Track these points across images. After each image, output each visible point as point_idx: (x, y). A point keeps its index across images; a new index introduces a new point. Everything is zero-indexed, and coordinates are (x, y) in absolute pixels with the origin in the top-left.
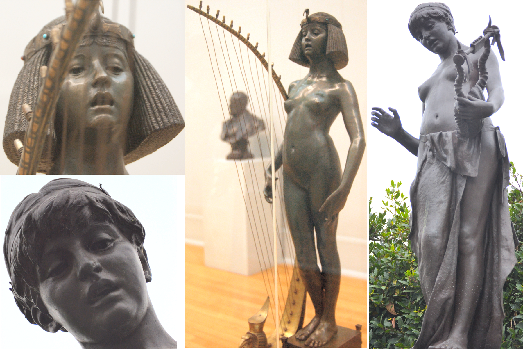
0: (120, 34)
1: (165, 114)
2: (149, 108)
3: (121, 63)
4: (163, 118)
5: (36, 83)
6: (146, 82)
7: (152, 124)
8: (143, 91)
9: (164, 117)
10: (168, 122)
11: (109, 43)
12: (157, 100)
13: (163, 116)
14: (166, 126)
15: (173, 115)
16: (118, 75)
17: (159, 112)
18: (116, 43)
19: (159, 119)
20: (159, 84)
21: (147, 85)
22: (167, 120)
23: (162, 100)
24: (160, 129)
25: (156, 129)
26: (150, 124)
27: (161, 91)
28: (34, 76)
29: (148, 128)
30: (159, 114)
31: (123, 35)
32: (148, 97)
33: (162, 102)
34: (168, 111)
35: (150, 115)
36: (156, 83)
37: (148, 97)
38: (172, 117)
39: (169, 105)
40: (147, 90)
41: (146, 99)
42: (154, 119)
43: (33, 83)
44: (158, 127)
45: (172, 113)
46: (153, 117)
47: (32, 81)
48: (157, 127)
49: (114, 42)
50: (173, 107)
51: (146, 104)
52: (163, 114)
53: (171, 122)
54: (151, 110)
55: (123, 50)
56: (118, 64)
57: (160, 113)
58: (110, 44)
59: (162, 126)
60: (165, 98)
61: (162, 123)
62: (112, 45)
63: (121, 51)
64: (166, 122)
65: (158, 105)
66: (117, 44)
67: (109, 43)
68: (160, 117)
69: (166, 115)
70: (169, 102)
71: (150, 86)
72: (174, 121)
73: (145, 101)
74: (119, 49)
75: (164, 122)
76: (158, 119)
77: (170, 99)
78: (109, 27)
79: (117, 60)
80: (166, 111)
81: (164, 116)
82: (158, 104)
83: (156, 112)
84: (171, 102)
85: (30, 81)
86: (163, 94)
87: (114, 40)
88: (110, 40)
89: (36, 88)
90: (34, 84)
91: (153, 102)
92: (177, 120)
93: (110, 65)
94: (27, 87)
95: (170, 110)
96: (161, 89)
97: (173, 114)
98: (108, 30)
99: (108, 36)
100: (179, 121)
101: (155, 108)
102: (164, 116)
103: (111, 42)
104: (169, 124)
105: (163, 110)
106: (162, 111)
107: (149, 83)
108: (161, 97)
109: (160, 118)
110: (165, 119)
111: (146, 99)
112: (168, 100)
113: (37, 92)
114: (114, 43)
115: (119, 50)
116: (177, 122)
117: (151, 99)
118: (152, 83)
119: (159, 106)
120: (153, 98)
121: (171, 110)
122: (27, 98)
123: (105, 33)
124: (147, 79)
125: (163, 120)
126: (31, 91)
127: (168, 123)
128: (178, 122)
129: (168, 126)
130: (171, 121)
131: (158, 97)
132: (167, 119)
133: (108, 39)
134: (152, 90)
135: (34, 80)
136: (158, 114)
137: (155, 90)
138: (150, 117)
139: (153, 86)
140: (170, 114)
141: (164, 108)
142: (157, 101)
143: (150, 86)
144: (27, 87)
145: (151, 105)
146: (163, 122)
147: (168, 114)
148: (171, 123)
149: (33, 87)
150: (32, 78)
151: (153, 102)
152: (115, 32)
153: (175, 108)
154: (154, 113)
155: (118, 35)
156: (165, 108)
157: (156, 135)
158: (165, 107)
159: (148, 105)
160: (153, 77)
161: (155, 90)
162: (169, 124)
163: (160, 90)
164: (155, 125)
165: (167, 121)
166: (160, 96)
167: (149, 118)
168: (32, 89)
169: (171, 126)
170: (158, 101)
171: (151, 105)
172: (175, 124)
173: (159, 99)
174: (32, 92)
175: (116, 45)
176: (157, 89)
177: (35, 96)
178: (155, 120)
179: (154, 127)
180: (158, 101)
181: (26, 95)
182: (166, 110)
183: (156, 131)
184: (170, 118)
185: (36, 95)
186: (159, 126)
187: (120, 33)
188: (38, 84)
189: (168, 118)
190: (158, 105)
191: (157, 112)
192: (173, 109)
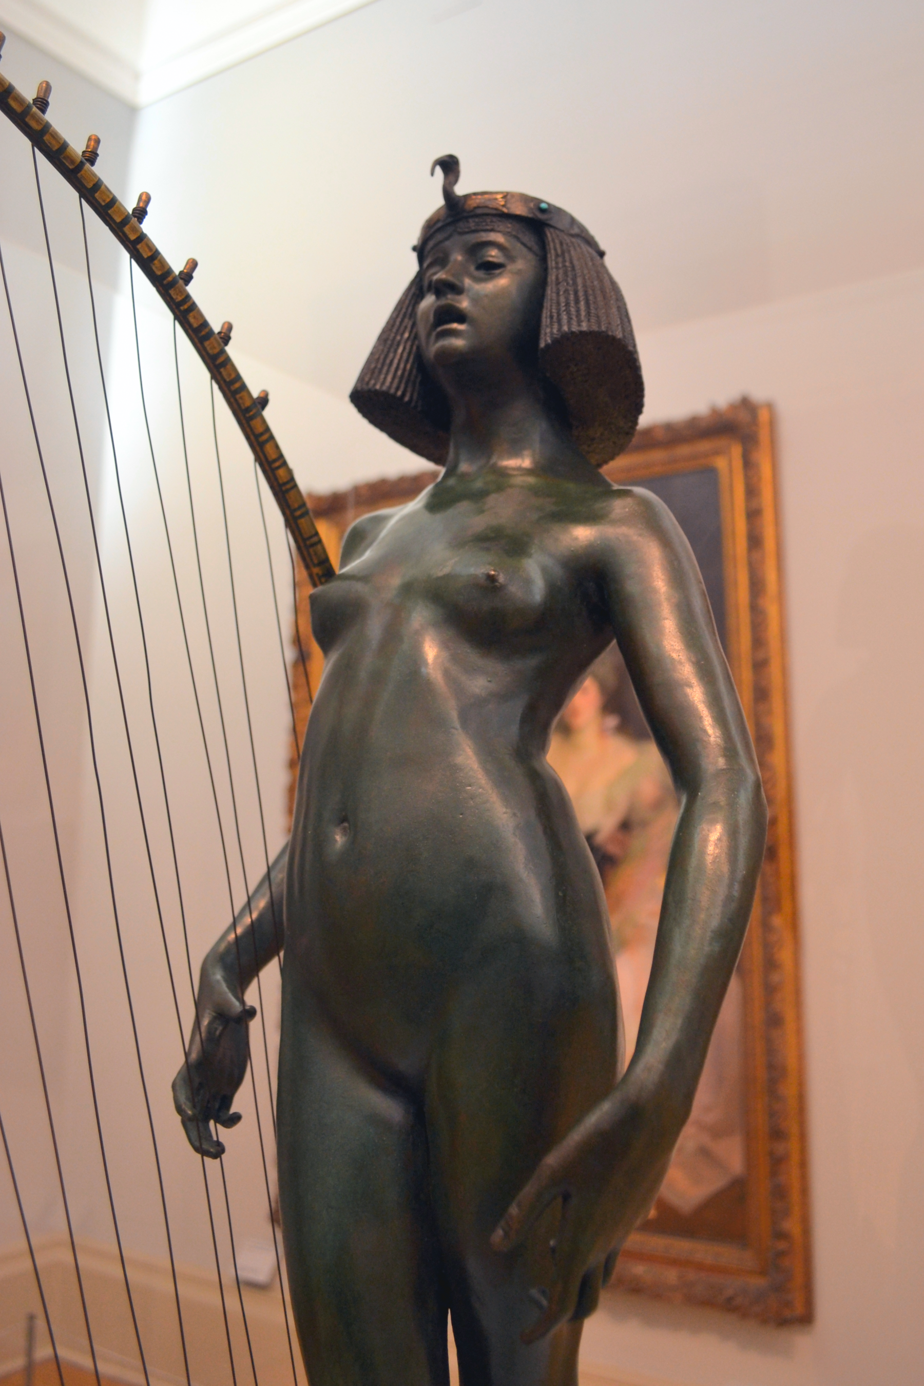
0: (501, 208)
55: (509, 232)
99: (477, 216)
123: (472, 211)
155: (496, 209)
175: (492, 227)
187: (503, 206)
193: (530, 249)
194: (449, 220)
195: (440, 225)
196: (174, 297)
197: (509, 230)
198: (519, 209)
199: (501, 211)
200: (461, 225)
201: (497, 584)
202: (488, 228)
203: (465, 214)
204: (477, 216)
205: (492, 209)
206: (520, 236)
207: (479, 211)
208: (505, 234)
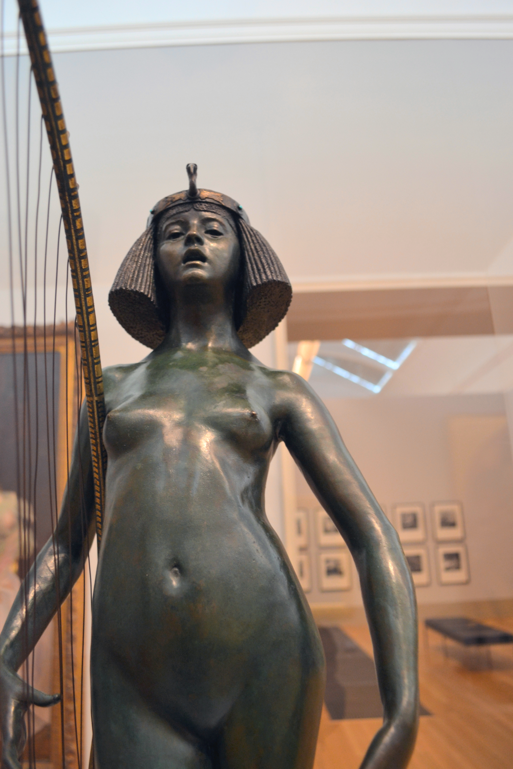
0: (221, 202)
6: (250, 246)
18: (216, 209)
21: (251, 249)
24: (258, 285)
32: (250, 259)
37: (250, 259)
40: (250, 253)
55: (224, 216)
73: (247, 263)
74: (219, 215)
87: (214, 207)
93: (208, 229)
107: (253, 247)
118: (255, 247)
120: (255, 259)
124: (252, 244)
137: (257, 252)
154: (254, 273)
155: (218, 202)
161: (257, 252)
187: (222, 201)
193: (233, 228)
194: (188, 201)
195: (182, 202)
196: (74, 205)
198: (229, 206)
201: (257, 419)
206: (229, 220)
207: (208, 200)
208: (223, 217)
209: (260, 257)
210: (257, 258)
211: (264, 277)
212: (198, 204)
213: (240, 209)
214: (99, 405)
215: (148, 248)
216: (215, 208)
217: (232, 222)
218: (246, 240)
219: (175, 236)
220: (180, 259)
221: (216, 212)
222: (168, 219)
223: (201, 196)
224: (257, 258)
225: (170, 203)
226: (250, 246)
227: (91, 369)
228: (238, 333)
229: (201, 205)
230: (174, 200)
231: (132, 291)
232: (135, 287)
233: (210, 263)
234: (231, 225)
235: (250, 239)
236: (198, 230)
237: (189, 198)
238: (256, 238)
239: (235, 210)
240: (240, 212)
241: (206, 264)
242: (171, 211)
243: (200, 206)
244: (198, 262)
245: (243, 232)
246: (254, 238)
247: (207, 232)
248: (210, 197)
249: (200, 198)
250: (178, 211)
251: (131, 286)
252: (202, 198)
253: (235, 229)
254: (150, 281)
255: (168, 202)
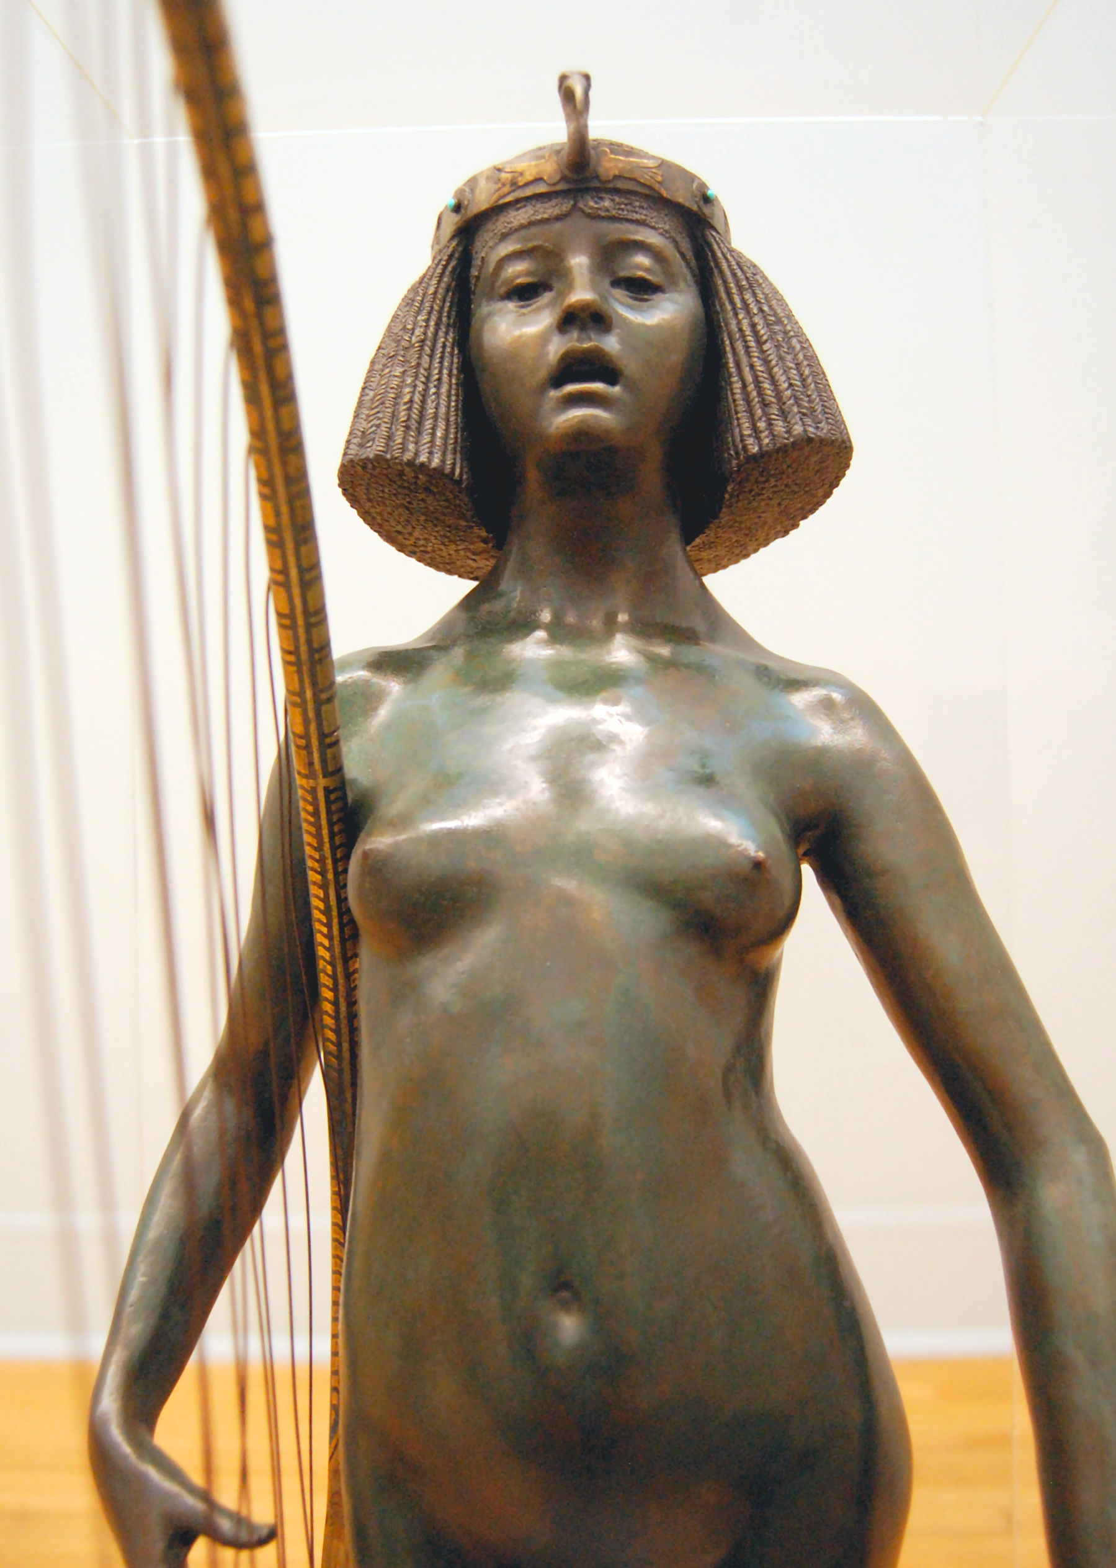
0: (657, 186)
1: (782, 410)
2: (737, 397)
3: (657, 268)
4: (773, 422)
5: (418, 331)
6: (739, 322)
7: (742, 441)
8: (728, 349)
9: (774, 420)
10: (786, 432)
11: (623, 210)
12: (762, 372)
13: (773, 417)
14: (778, 445)
15: (804, 414)
16: (646, 300)
17: (765, 405)
18: (645, 212)
19: (762, 425)
20: (777, 328)
21: (741, 330)
22: (784, 427)
23: (776, 373)
24: (762, 454)
25: (749, 453)
26: (738, 439)
27: (778, 347)
28: (418, 313)
29: (732, 452)
30: (763, 411)
31: (667, 189)
33: (777, 378)
34: (792, 401)
35: (739, 415)
36: (768, 325)
38: (801, 419)
39: (797, 386)
40: (739, 346)
41: (733, 370)
42: (747, 425)
43: (411, 332)
44: (756, 449)
45: (802, 409)
46: (745, 420)
47: (409, 327)
48: (754, 449)
49: (637, 209)
50: (809, 393)
51: (731, 384)
52: (774, 410)
53: (795, 433)
54: (743, 400)
55: (666, 231)
56: (647, 270)
57: (766, 409)
58: (625, 213)
59: (768, 444)
60: (787, 367)
61: (767, 437)
62: (629, 217)
63: (661, 234)
64: (780, 431)
65: (762, 385)
66: (646, 215)
67: (623, 210)
68: (764, 419)
69: (784, 414)
70: (797, 378)
71: (748, 332)
72: (805, 431)
73: (730, 376)
74: (653, 228)
75: (776, 433)
76: (759, 424)
77: (803, 369)
78: (620, 165)
79: (642, 260)
80: (784, 403)
81: (777, 415)
82: (763, 382)
83: (755, 406)
84: (804, 377)
85: (404, 328)
86: (783, 354)
87: (637, 204)
88: (626, 202)
89: (417, 345)
90: (413, 334)
91: (749, 378)
92: (817, 428)
93: (623, 274)
94: (395, 343)
95: (796, 398)
96: (778, 341)
97: (804, 411)
98: (617, 173)
99: (617, 191)
100: (825, 431)
101: (754, 394)
102: (777, 418)
103: (629, 207)
104: (787, 439)
105: (773, 400)
106: (773, 403)
108: (774, 363)
109: (765, 421)
110: (777, 426)
111: (733, 370)
112: (795, 372)
113: (417, 356)
114: (636, 212)
115: (653, 232)
116: (815, 434)
117: (746, 370)
118: (753, 326)
119: (765, 389)
120: (752, 367)
121: (801, 399)
122: (390, 372)
123: (610, 181)
125: (772, 427)
126: (402, 353)
127: (786, 436)
128: (819, 434)
129: (785, 445)
130: (796, 430)
131: (766, 362)
132: (786, 424)
133: (617, 199)
134: (752, 344)
135: (415, 324)
136: (759, 412)
137: (760, 343)
138: (738, 419)
139: (756, 333)
140: (795, 409)
141: (778, 394)
142: (761, 374)
143: (748, 332)
144: (395, 345)
145: (744, 386)
146: (772, 434)
147: (787, 409)
148: (794, 436)
149: (410, 341)
150: (411, 320)
151: (749, 378)
152: (642, 181)
153: (816, 393)
155: (651, 188)
156: (782, 394)
157: (756, 473)
158: (781, 392)
159: (737, 386)
160: (761, 310)
161: (760, 343)
162: (787, 439)
163: (776, 344)
164: (751, 441)
165: (784, 430)
166: (770, 361)
167: (735, 423)
168: (406, 348)
169: (793, 443)
170: (763, 376)
171: (744, 386)
172: (810, 440)
173: (770, 370)
174: (403, 356)
175: (643, 217)
176: (766, 341)
177: (412, 366)
178: (751, 430)
179: (745, 448)
180: (763, 376)
181: (389, 365)
182: (784, 399)
183: (754, 458)
184: (793, 421)
185: (413, 364)
186: (760, 446)
187: (659, 183)
188: (425, 333)
189: (789, 422)
190: (762, 385)
191: (758, 405)
192: (809, 396)
193: (688, 263)
194: (561, 187)
195: (542, 188)
197: (667, 227)
198: (681, 197)
199: (659, 193)
200: (590, 203)
202: (636, 216)
203: (596, 184)
204: (617, 191)
205: (644, 185)
207: (620, 185)
208: (664, 234)
209: (766, 362)
210: (758, 363)
211: (780, 427)
212: (593, 198)
213: (707, 200)
214: (332, 797)
215: (444, 319)
216: (641, 207)
217: (686, 245)
218: (724, 296)
219: (525, 293)
220: (543, 373)
221: (645, 221)
222: (504, 237)
223: (601, 171)
224: (759, 367)
225: (506, 189)
226: (736, 323)
227: (311, 714)
228: (688, 548)
229: (602, 199)
230: (521, 181)
231: (410, 463)
232: (417, 454)
233: (630, 387)
234: (683, 255)
235: (737, 299)
236: (594, 286)
237: (564, 178)
238: (754, 295)
239: (695, 208)
240: (706, 210)
241: (616, 390)
242: (513, 213)
243: (596, 203)
244: (598, 386)
245: (716, 271)
246: (748, 296)
247: (617, 282)
248: (626, 175)
249: (597, 177)
250: (533, 218)
251: (404, 449)
252: (604, 178)
253: (693, 263)
254: (456, 423)
255: (504, 185)
